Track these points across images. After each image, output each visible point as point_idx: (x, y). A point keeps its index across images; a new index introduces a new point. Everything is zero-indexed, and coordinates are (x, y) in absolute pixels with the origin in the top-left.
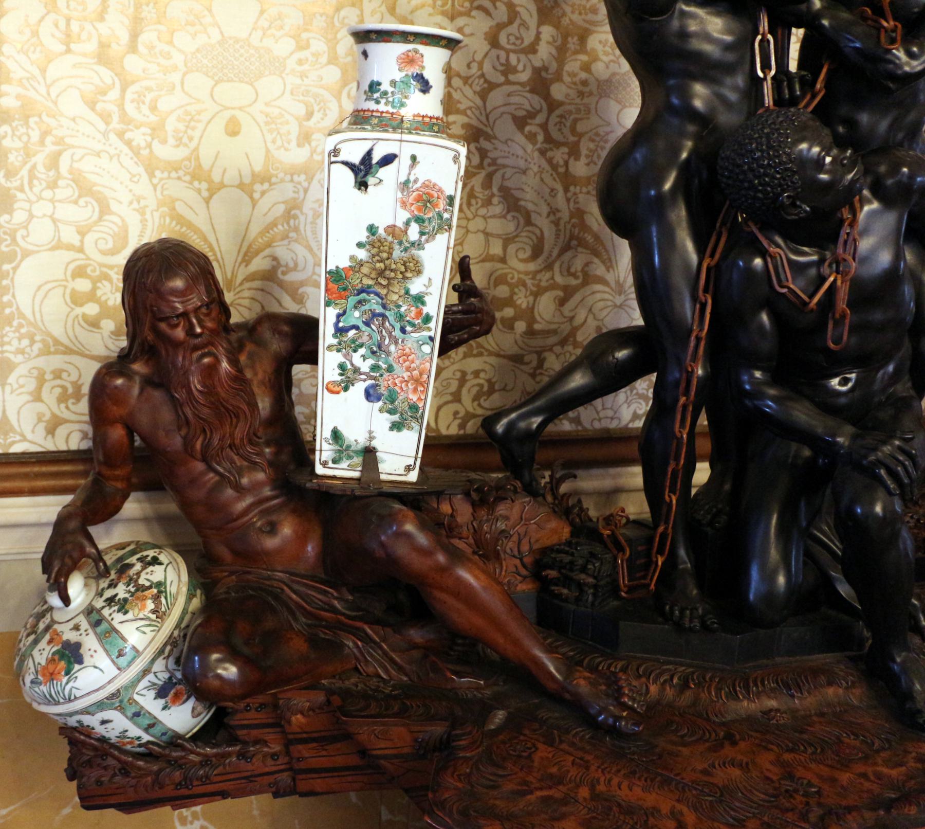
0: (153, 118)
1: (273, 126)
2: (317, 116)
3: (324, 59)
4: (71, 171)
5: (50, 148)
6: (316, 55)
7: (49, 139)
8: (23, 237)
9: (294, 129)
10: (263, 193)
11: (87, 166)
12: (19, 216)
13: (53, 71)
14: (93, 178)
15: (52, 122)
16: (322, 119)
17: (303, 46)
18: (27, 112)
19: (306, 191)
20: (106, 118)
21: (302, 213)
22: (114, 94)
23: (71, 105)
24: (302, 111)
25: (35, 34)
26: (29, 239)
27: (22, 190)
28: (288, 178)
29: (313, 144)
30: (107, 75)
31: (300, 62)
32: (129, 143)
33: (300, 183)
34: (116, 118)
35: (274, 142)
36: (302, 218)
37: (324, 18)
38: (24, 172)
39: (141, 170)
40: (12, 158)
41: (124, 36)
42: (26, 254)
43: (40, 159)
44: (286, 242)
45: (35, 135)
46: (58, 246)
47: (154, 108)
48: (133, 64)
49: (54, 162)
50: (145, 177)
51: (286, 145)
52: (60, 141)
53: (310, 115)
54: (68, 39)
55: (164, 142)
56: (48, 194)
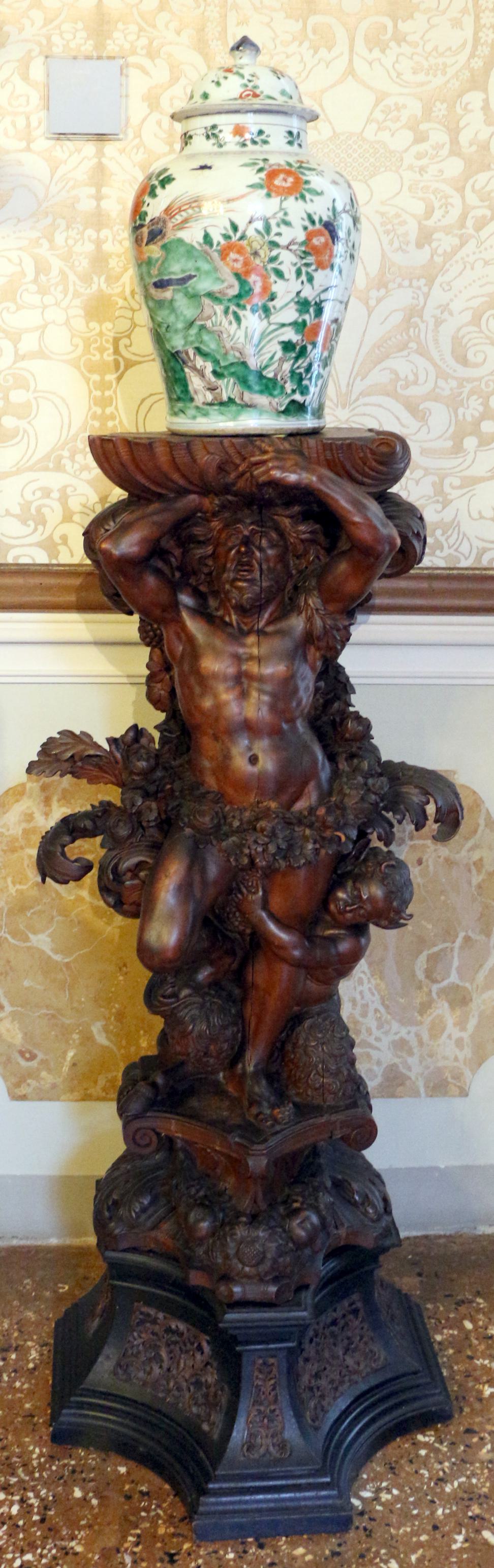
1: (389, 227)
2: (438, 214)
3: (445, 152)
6: (438, 147)
8: (126, 346)
9: (412, 228)
10: (379, 301)
16: (443, 216)
17: (420, 138)
19: (427, 296)
21: (423, 322)
24: (419, 208)
26: (131, 349)
28: (406, 283)
29: (434, 245)
31: (419, 156)
33: (419, 288)
35: (391, 243)
36: (422, 326)
37: (445, 105)
40: (113, 263)
44: (405, 353)
51: (404, 247)
53: (429, 212)
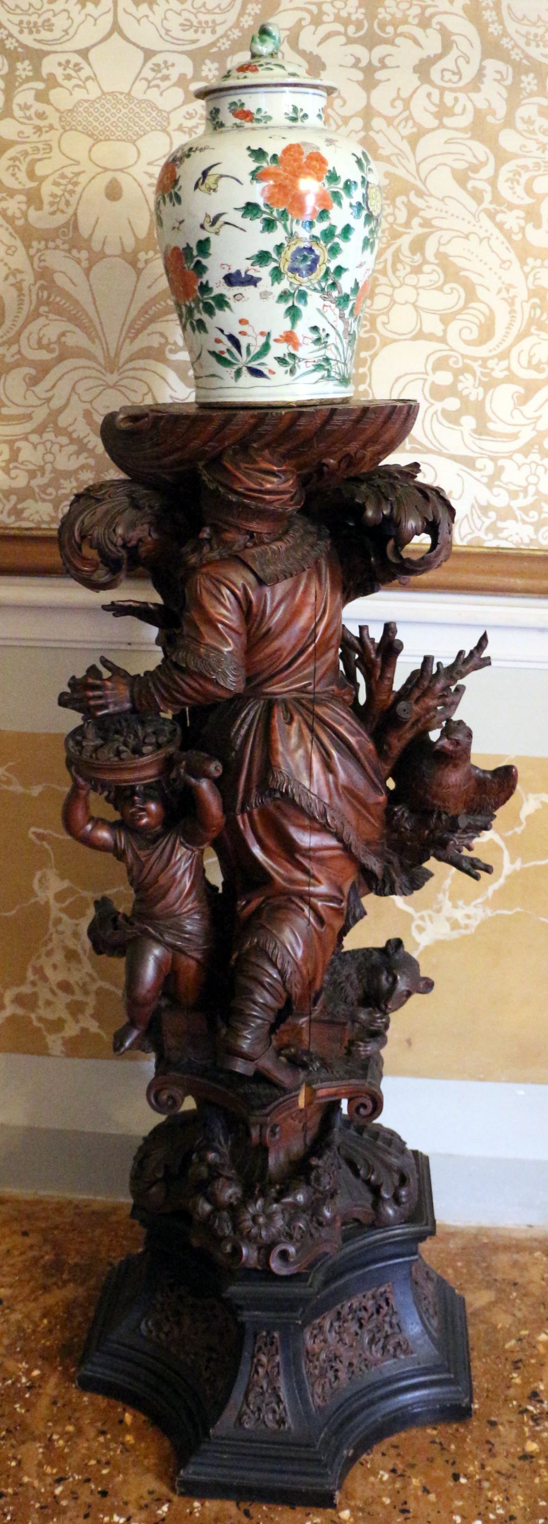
0: (528, 200)
4: (438, 254)
5: (416, 230)
7: (416, 221)
11: (455, 249)
13: (427, 145)
14: (460, 262)
15: (418, 202)
20: (476, 195)
22: (487, 172)
23: (441, 182)
30: (481, 150)
32: (500, 226)
34: (488, 197)
39: (512, 256)
41: (501, 109)
42: (386, 342)
43: (405, 242)
45: (402, 216)
47: (529, 190)
48: (508, 140)
49: (418, 245)
50: (516, 264)
52: (426, 223)
54: (443, 112)
56: (412, 279)
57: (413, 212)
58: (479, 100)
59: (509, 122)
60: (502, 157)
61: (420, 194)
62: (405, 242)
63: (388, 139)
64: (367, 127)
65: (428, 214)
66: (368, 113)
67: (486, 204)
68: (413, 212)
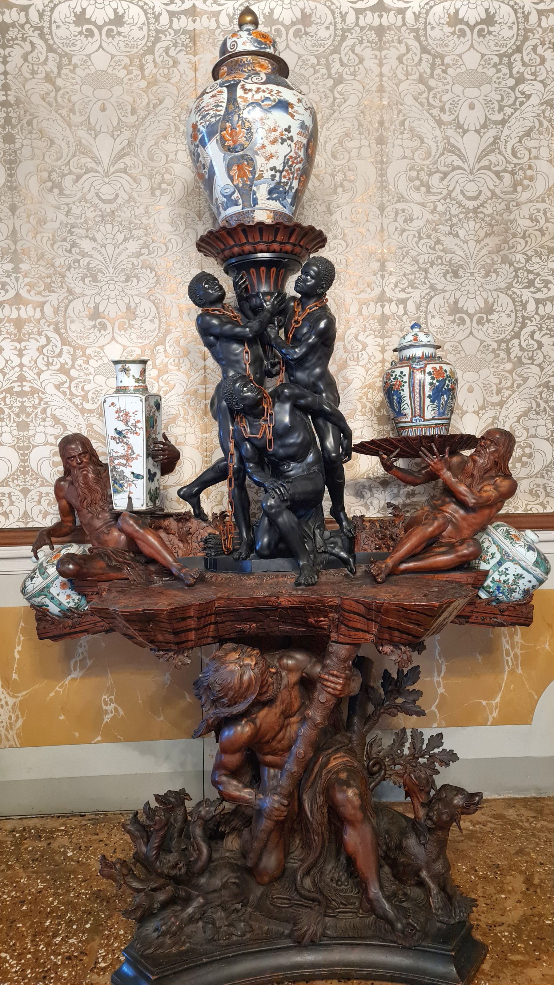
0: (83, 393)
4: (51, 415)
5: (43, 406)
7: (42, 403)
11: (57, 412)
12: (31, 432)
14: (60, 417)
18: (34, 391)
20: (64, 393)
23: (50, 389)
25: (35, 362)
27: (32, 422)
30: (64, 378)
32: (74, 403)
38: (33, 415)
42: (34, 447)
43: (39, 410)
45: (37, 402)
46: (47, 443)
49: (44, 411)
52: (46, 403)
55: (88, 402)
56: (42, 424)
57: (41, 399)
58: (62, 360)
59: (73, 367)
60: (72, 379)
61: (43, 393)
62: (39, 410)
63: (30, 375)
64: (21, 370)
65: (46, 400)
66: (21, 365)
67: (68, 396)
68: (41, 399)
